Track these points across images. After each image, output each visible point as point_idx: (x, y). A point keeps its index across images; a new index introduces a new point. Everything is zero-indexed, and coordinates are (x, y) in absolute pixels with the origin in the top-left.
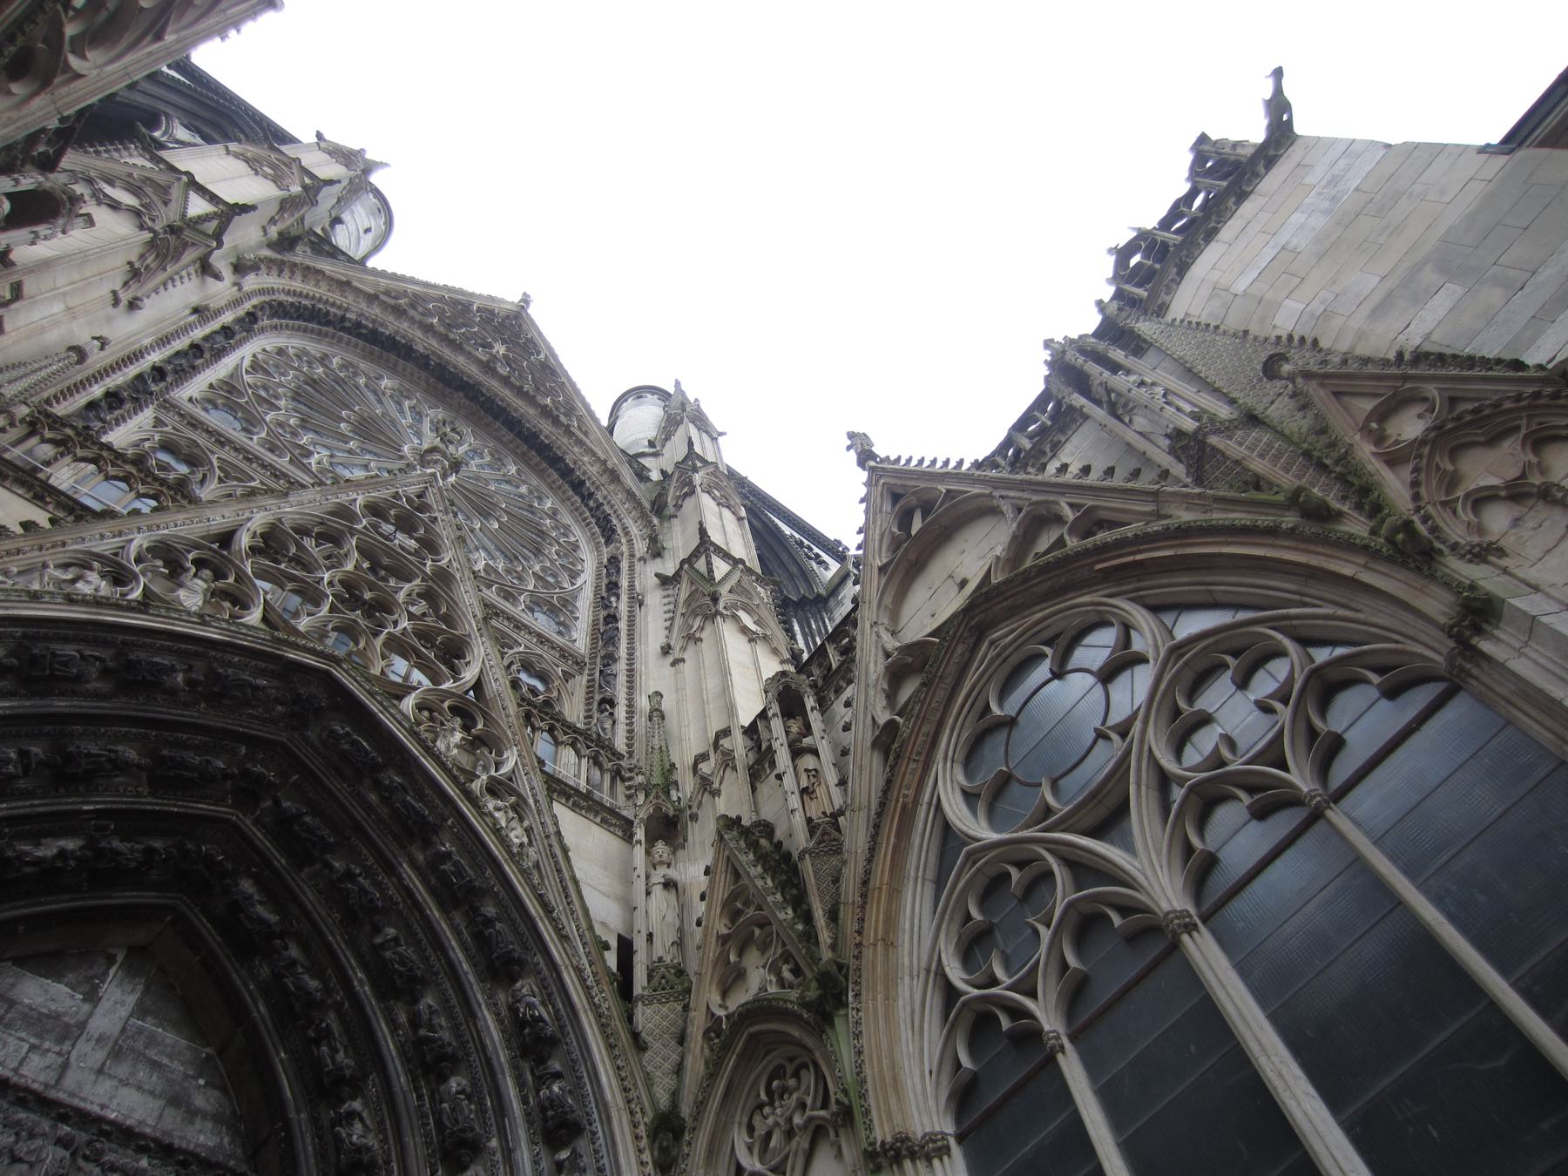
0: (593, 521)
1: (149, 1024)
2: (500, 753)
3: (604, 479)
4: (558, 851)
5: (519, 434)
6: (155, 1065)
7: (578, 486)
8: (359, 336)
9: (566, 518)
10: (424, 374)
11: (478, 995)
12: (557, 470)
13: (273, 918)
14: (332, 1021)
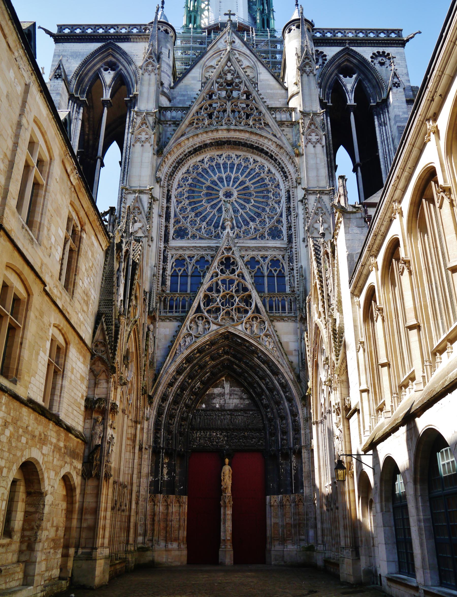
0: (280, 169)
1: (233, 388)
2: (264, 324)
3: (278, 149)
4: (280, 345)
5: (248, 147)
6: (236, 394)
7: (271, 157)
8: (192, 154)
9: (273, 170)
10: (214, 147)
11: (273, 378)
12: (264, 153)
13: (240, 371)
14: (255, 385)
